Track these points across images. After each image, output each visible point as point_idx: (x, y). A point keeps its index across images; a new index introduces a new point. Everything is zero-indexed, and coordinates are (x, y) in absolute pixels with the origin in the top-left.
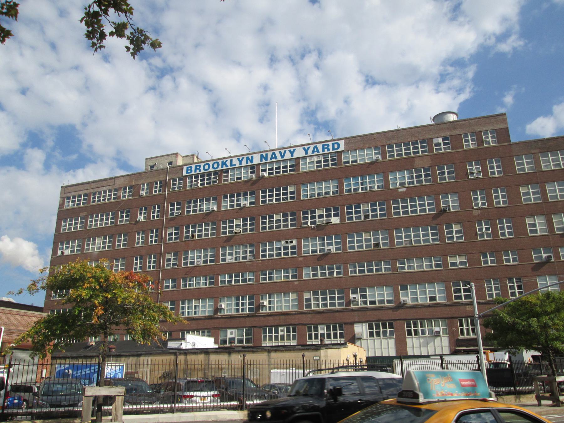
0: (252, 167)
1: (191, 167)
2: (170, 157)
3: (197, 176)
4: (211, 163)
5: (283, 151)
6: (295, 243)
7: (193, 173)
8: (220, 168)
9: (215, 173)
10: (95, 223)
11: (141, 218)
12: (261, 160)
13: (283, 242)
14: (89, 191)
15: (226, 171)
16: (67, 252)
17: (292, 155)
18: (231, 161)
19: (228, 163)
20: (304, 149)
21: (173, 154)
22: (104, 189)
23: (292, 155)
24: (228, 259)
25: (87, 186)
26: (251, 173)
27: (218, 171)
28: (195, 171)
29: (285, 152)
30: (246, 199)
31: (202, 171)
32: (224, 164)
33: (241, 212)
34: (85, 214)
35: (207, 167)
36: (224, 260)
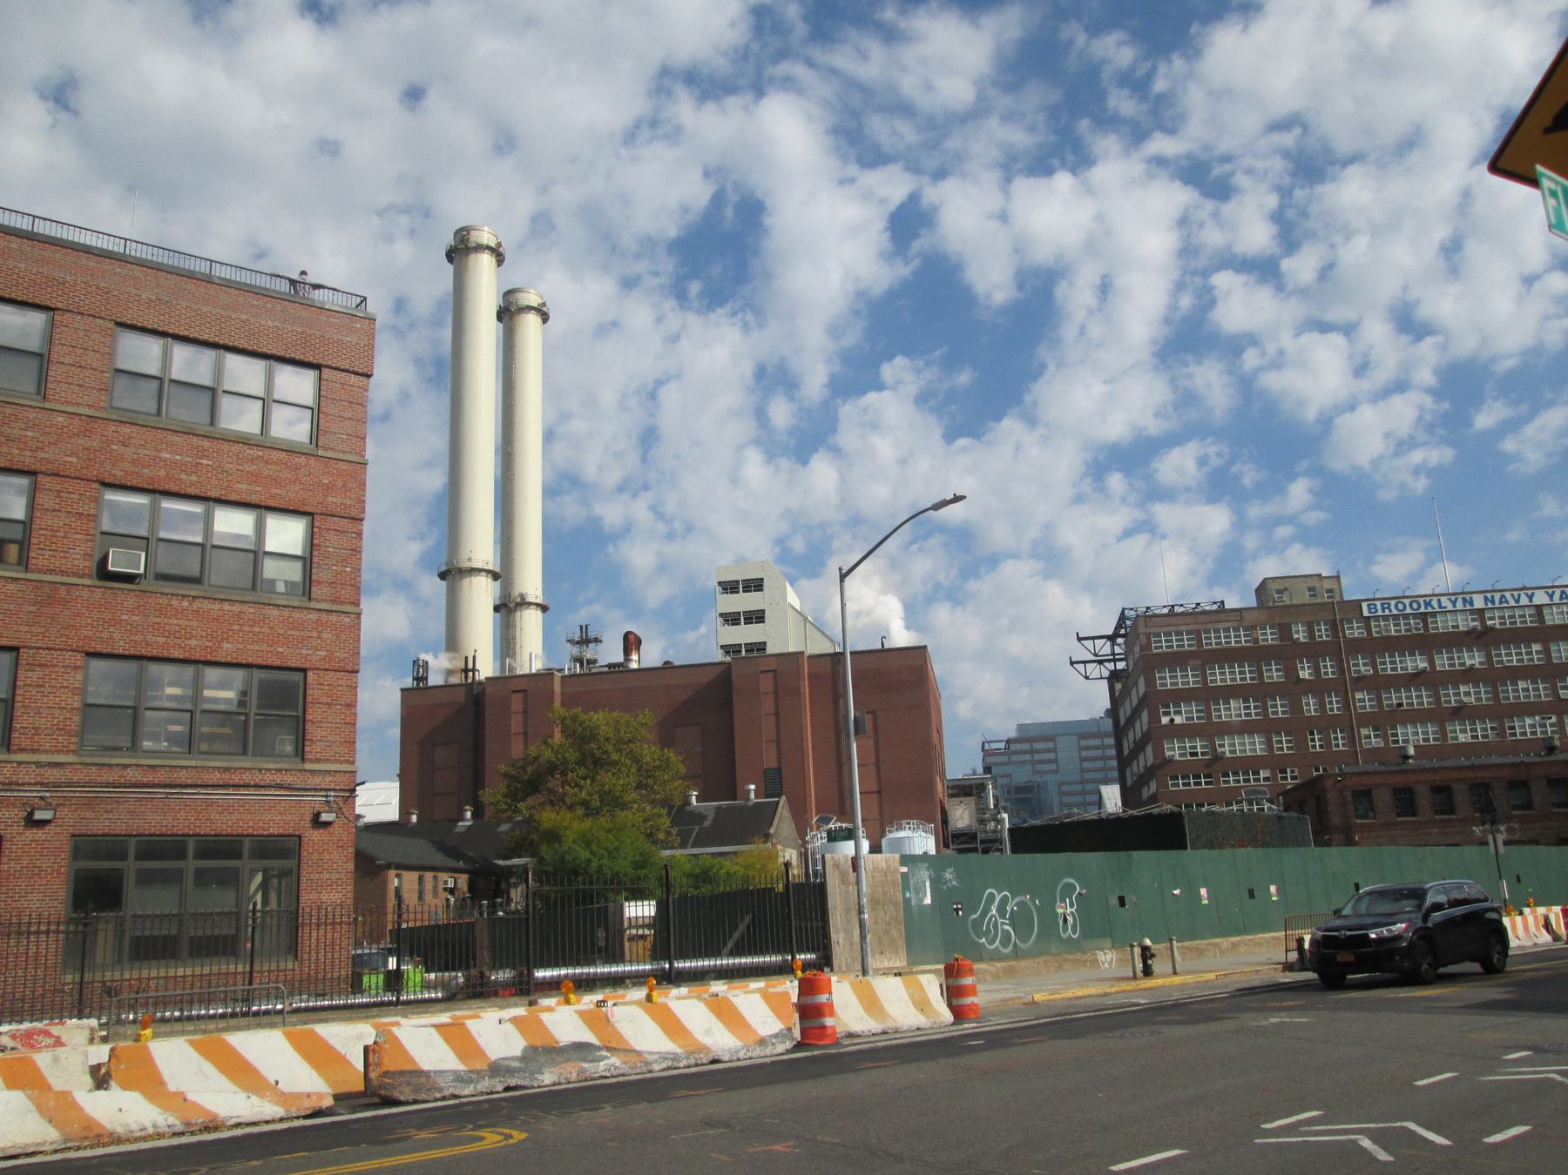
0: (1472, 612)
1: (1375, 605)
2: (1308, 579)
3: (1385, 618)
4: (1407, 601)
5: (1516, 593)
6: (1554, 719)
7: (1380, 613)
8: (1422, 610)
9: (1415, 616)
10: (1221, 676)
11: (1305, 674)
12: (1486, 604)
13: (1537, 718)
14: (1196, 627)
15: (1434, 614)
16: (1178, 720)
17: (1531, 601)
18: (1439, 601)
19: (1435, 603)
20: (1547, 593)
21: (1315, 575)
22: (1225, 625)
23: (1531, 601)
24: (1462, 738)
25: (1188, 619)
26: (1473, 620)
27: (1422, 613)
28: (1383, 611)
29: (1519, 595)
30: (1472, 657)
31: (1395, 612)
32: (1428, 604)
33: (1468, 675)
34: (1198, 662)
35: (1400, 606)
36: (1456, 738)
